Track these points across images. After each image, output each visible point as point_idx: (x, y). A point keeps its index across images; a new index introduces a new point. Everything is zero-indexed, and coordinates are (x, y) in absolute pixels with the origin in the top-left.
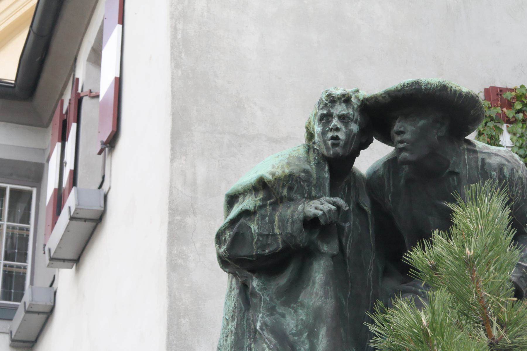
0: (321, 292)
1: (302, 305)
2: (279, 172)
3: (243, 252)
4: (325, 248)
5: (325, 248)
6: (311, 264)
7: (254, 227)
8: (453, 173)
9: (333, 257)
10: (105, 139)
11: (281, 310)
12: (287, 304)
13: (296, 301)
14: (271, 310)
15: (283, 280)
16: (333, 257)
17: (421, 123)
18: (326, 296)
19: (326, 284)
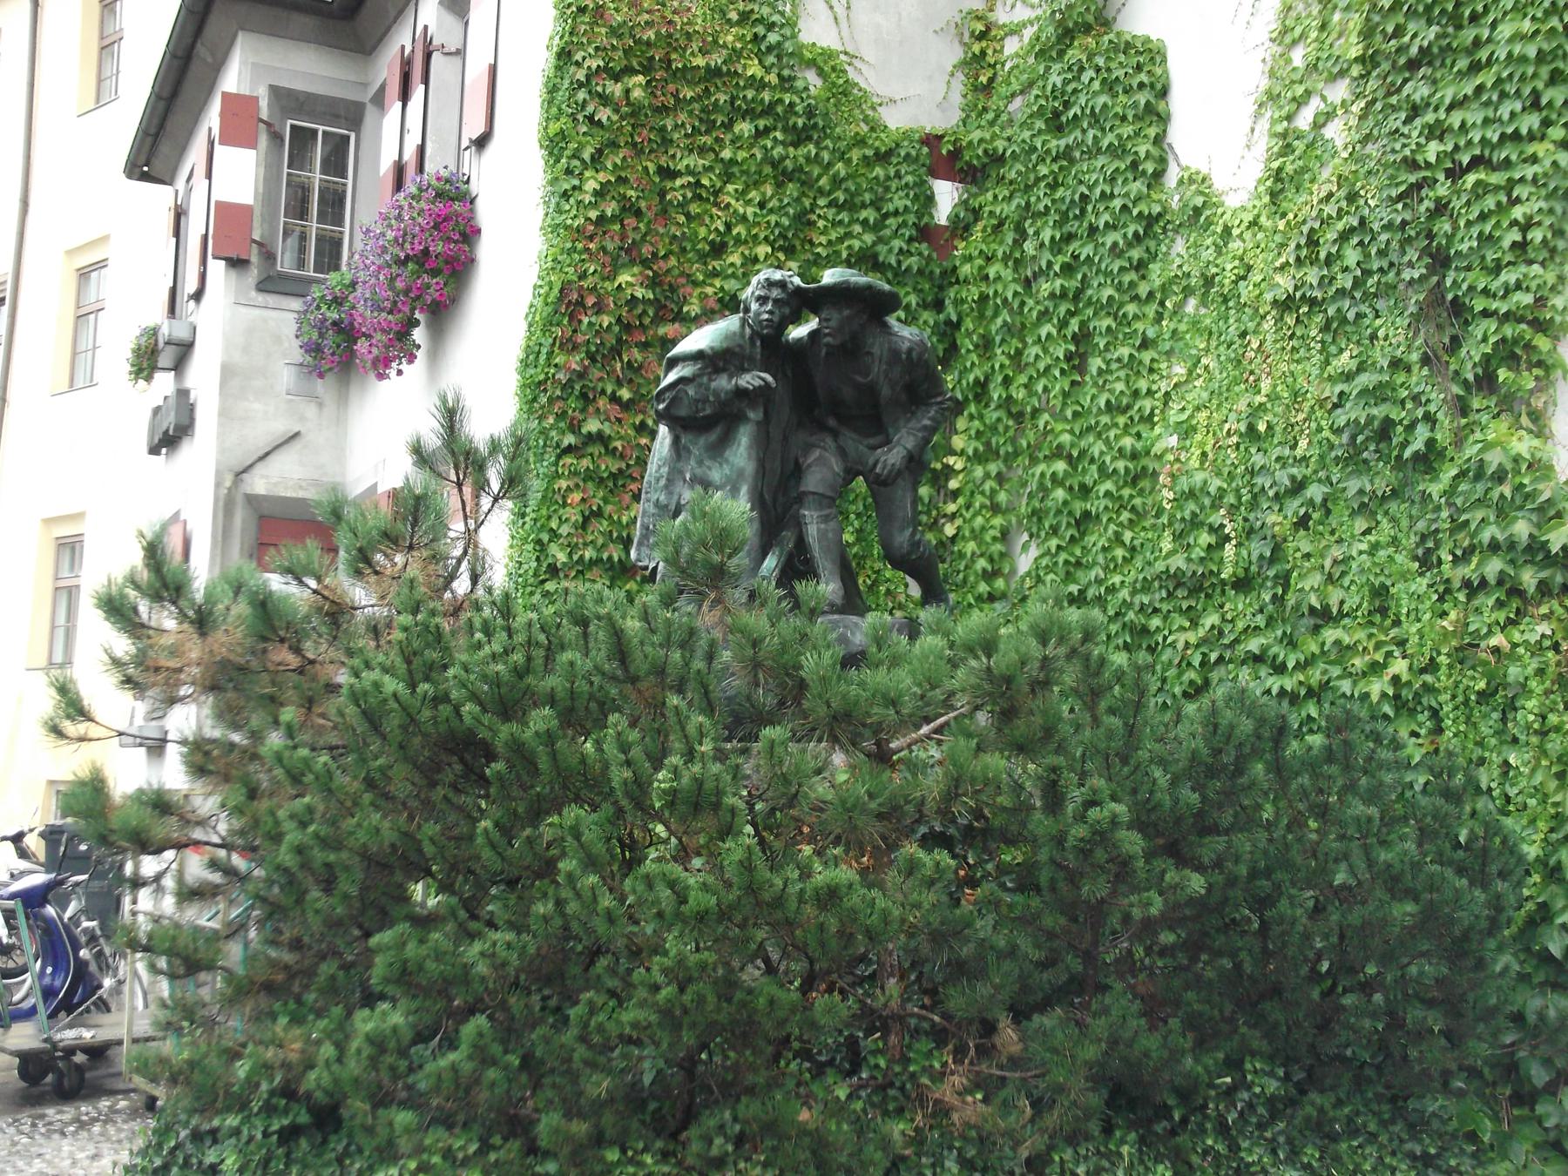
0: (745, 454)
1: (727, 461)
2: (716, 344)
3: (683, 412)
4: (751, 415)
5: (751, 415)
6: (738, 427)
7: (691, 392)
8: (869, 353)
9: (758, 423)
10: (474, 137)
11: (707, 463)
12: (713, 458)
13: (721, 455)
14: (700, 463)
15: (713, 436)
16: (758, 423)
17: (846, 312)
18: (749, 458)
19: (750, 447)
